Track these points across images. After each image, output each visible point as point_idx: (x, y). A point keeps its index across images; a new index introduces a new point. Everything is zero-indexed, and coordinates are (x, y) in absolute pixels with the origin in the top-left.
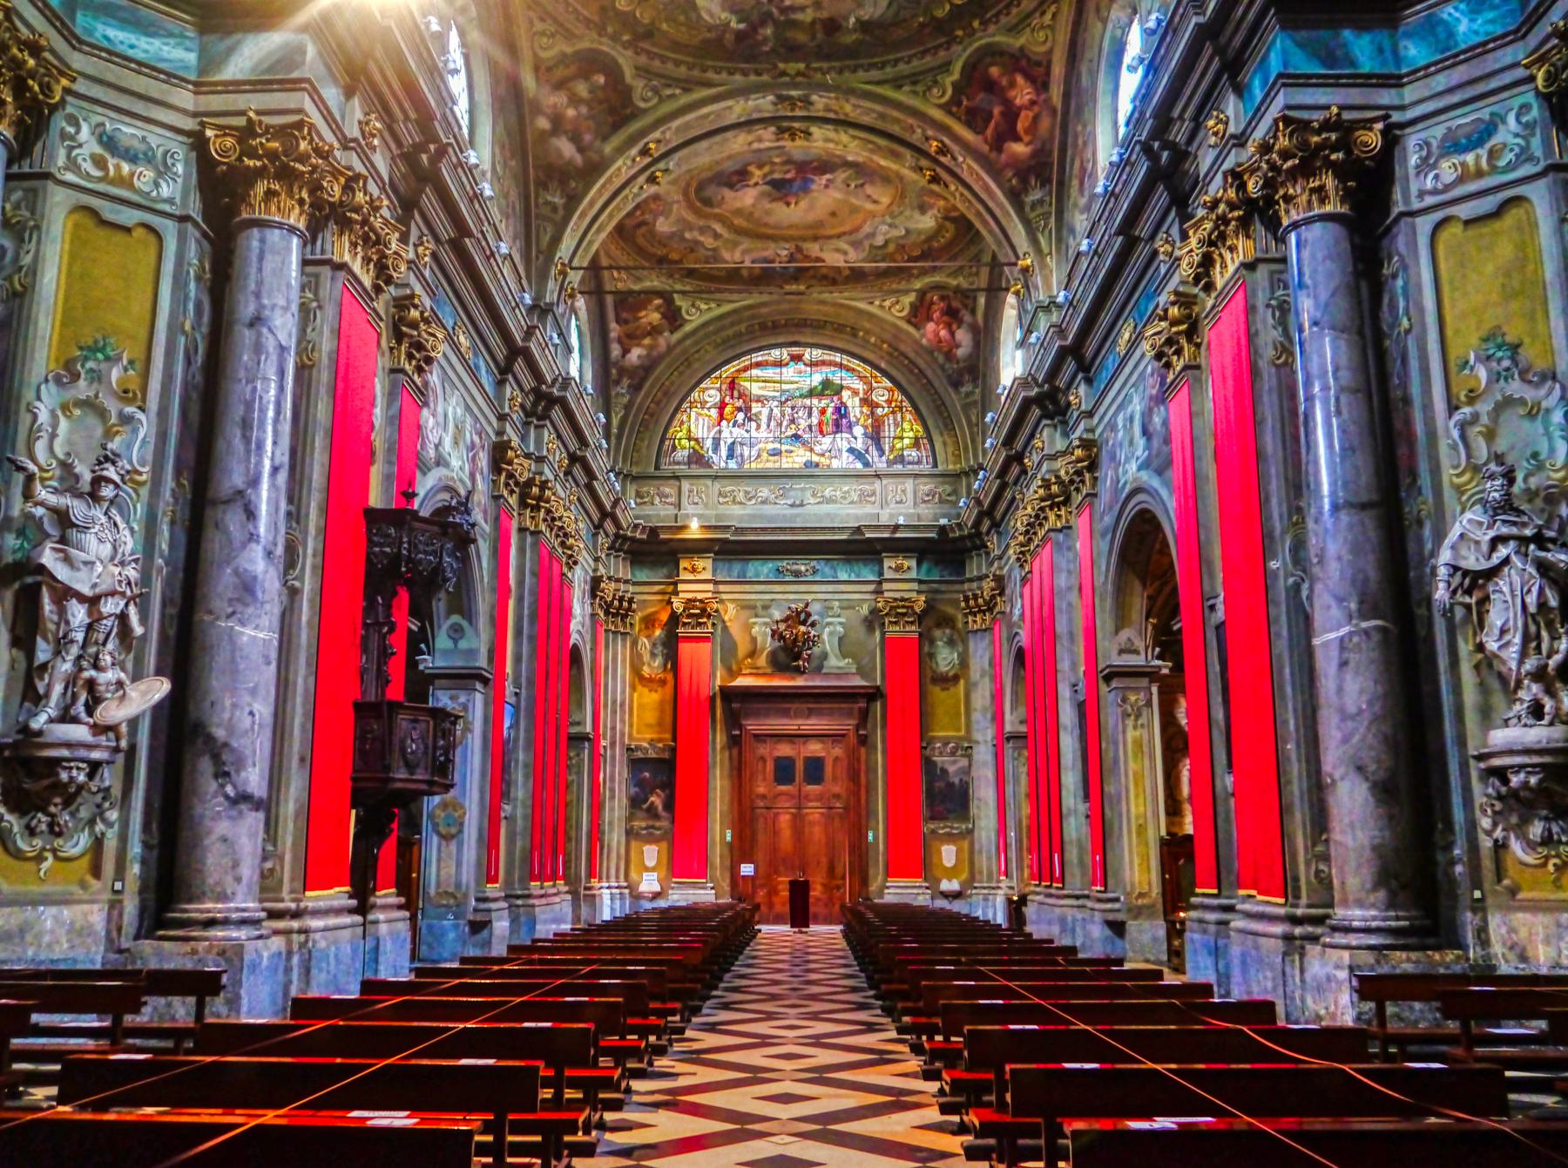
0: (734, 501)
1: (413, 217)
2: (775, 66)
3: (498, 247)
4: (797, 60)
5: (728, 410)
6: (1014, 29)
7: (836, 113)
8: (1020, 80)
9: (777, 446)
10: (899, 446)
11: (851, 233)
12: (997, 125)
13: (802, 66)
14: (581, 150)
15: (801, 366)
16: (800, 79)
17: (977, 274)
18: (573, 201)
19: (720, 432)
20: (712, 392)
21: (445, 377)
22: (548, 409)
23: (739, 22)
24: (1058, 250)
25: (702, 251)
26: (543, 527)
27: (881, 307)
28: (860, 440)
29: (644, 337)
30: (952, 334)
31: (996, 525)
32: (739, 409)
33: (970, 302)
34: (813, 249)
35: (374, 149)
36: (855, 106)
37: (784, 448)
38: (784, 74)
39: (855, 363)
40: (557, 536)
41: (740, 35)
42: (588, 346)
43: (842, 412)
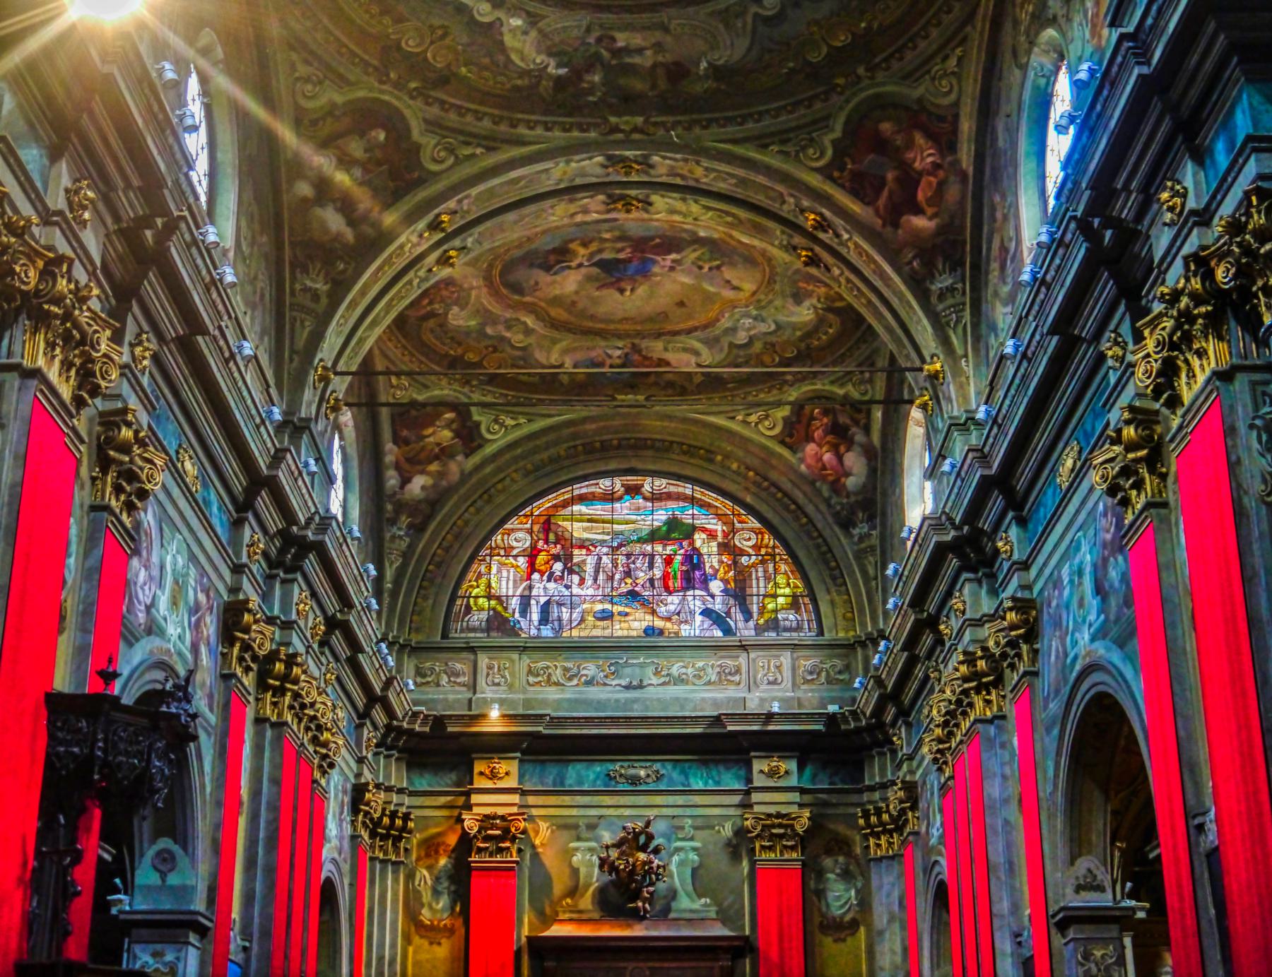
0: (549, 682)
1: (130, 309)
2: (606, 121)
3: (240, 347)
4: (633, 114)
5: (541, 558)
6: (910, 77)
7: (683, 177)
8: (919, 139)
9: (609, 606)
10: (770, 606)
11: (705, 327)
12: (891, 193)
13: (639, 120)
14: (351, 223)
15: (639, 501)
16: (636, 136)
17: (871, 381)
18: (340, 287)
19: (530, 588)
20: (520, 535)
21: (164, 517)
22: (300, 557)
23: (559, 66)
24: (976, 350)
25: (509, 349)
26: (288, 717)
28: (718, 600)
29: (430, 462)
30: (840, 458)
31: (904, 713)
32: (556, 558)
33: (861, 417)
34: (656, 348)
35: (84, 224)
36: (707, 169)
37: (617, 609)
38: (615, 129)
39: (711, 497)
40: (308, 729)
41: (559, 82)
42: (355, 473)
43: (693, 561)
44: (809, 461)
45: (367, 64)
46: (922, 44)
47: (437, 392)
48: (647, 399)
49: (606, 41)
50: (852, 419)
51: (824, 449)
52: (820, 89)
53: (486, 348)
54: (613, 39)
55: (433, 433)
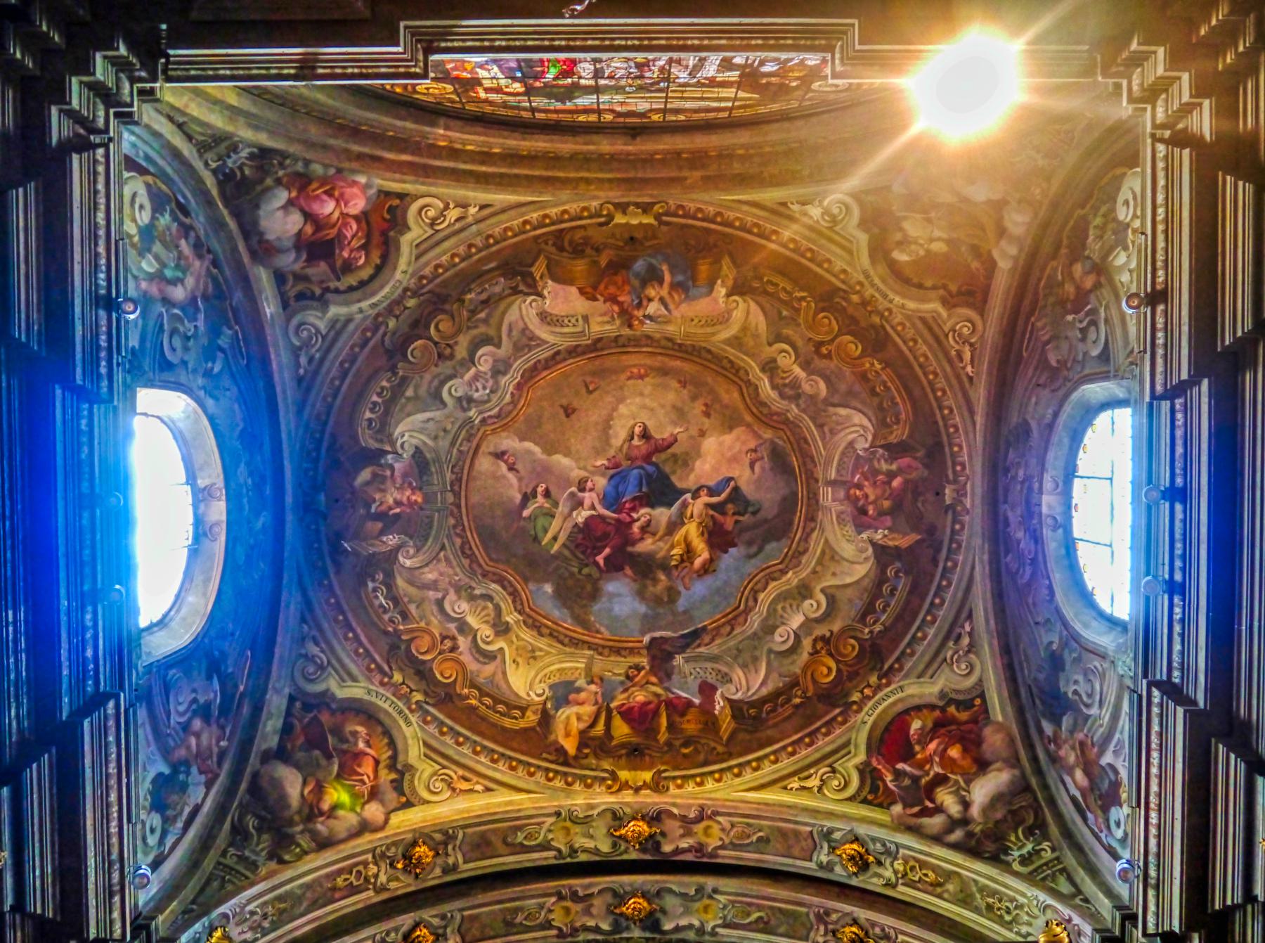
7: (575, 897)
17: (296, 352)
27: (465, 206)
30: (308, 216)
33: (292, 289)
34: (602, 323)
36: (548, 925)
44: (355, 190)
47: (911, 305)
48: (610, 217)
50: (306, 278)
51: (336, 215)
53: (828, 356)
55: (932, 240)
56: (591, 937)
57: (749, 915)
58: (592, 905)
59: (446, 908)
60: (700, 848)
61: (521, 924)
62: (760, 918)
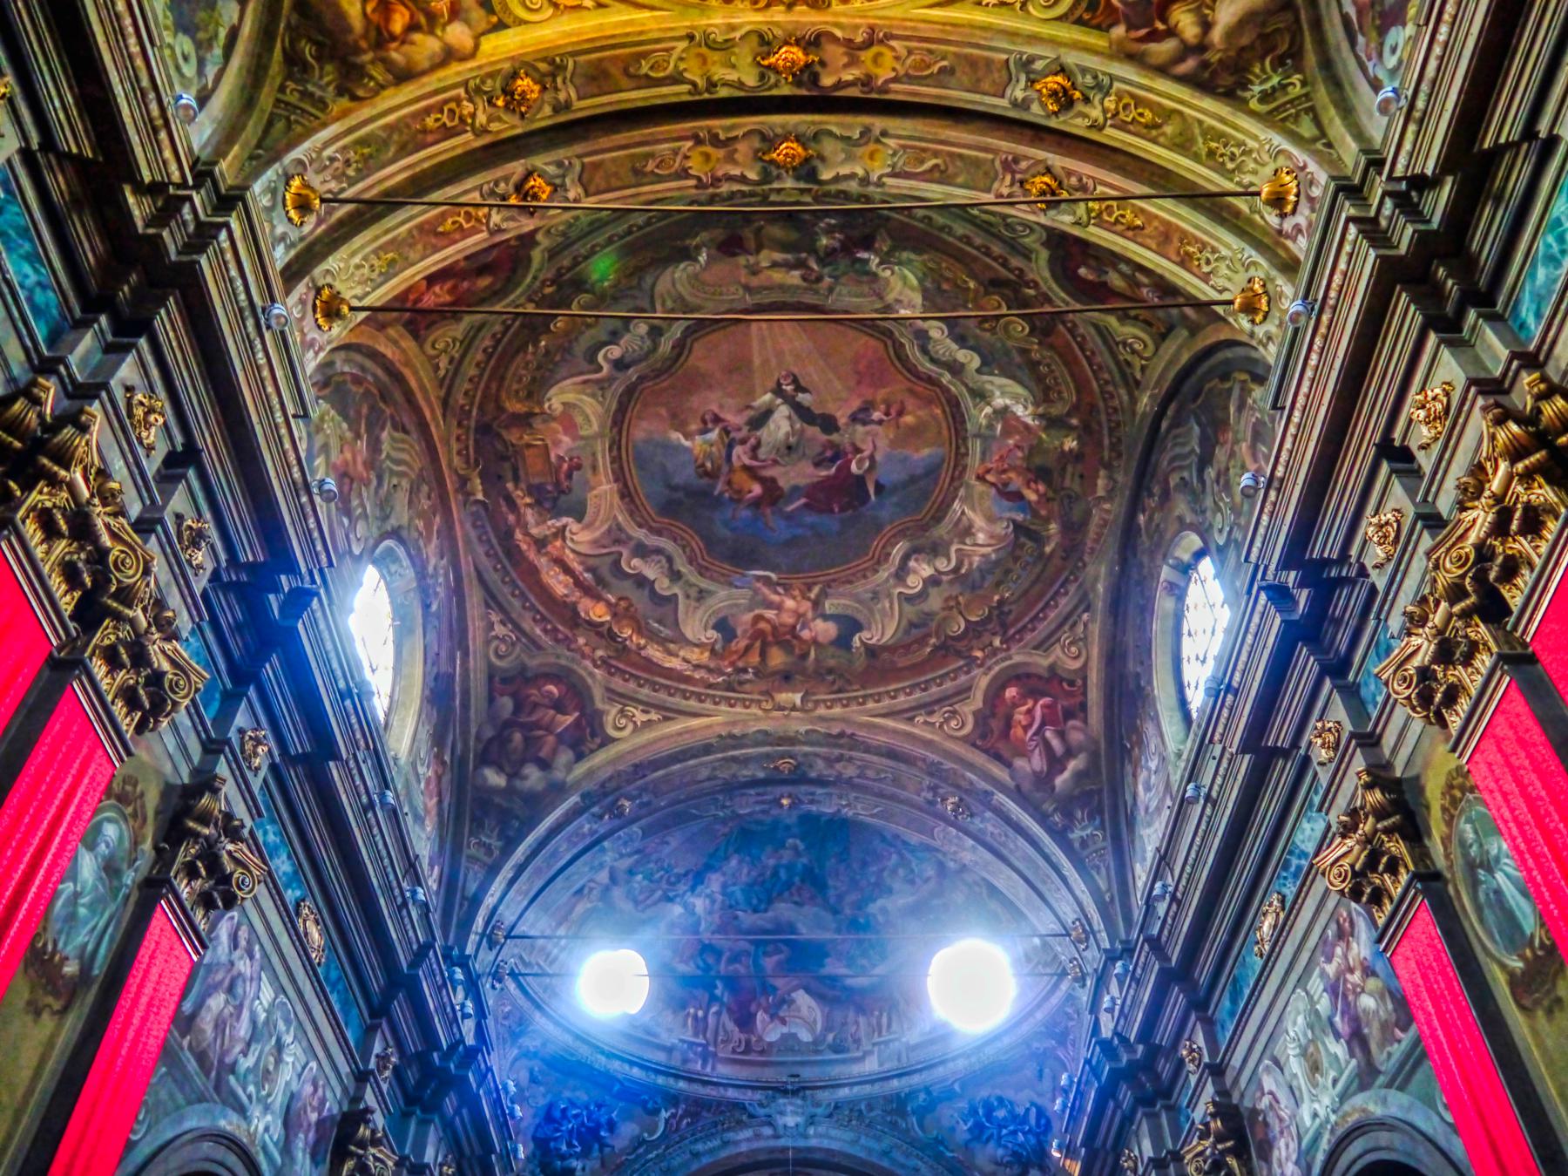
7: (715, 141)
23: (867, 261)
36: (684, 174)
41: (867, 243)
45: (1070, 331)
46: (480, 356)
49: (813, 277)
52: (568, 276)
54: (804, 278)
56: (736, 187)
57: (922, 162)
58: (736, 150)
59: (561, 153)
60: (867, 82)
61: (652, 172)
62: (936, 166)
